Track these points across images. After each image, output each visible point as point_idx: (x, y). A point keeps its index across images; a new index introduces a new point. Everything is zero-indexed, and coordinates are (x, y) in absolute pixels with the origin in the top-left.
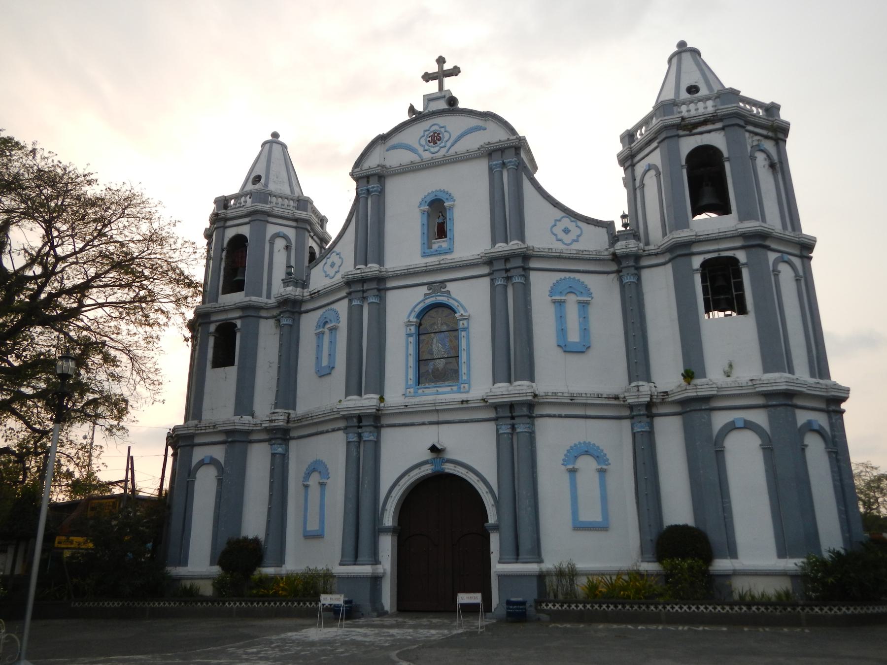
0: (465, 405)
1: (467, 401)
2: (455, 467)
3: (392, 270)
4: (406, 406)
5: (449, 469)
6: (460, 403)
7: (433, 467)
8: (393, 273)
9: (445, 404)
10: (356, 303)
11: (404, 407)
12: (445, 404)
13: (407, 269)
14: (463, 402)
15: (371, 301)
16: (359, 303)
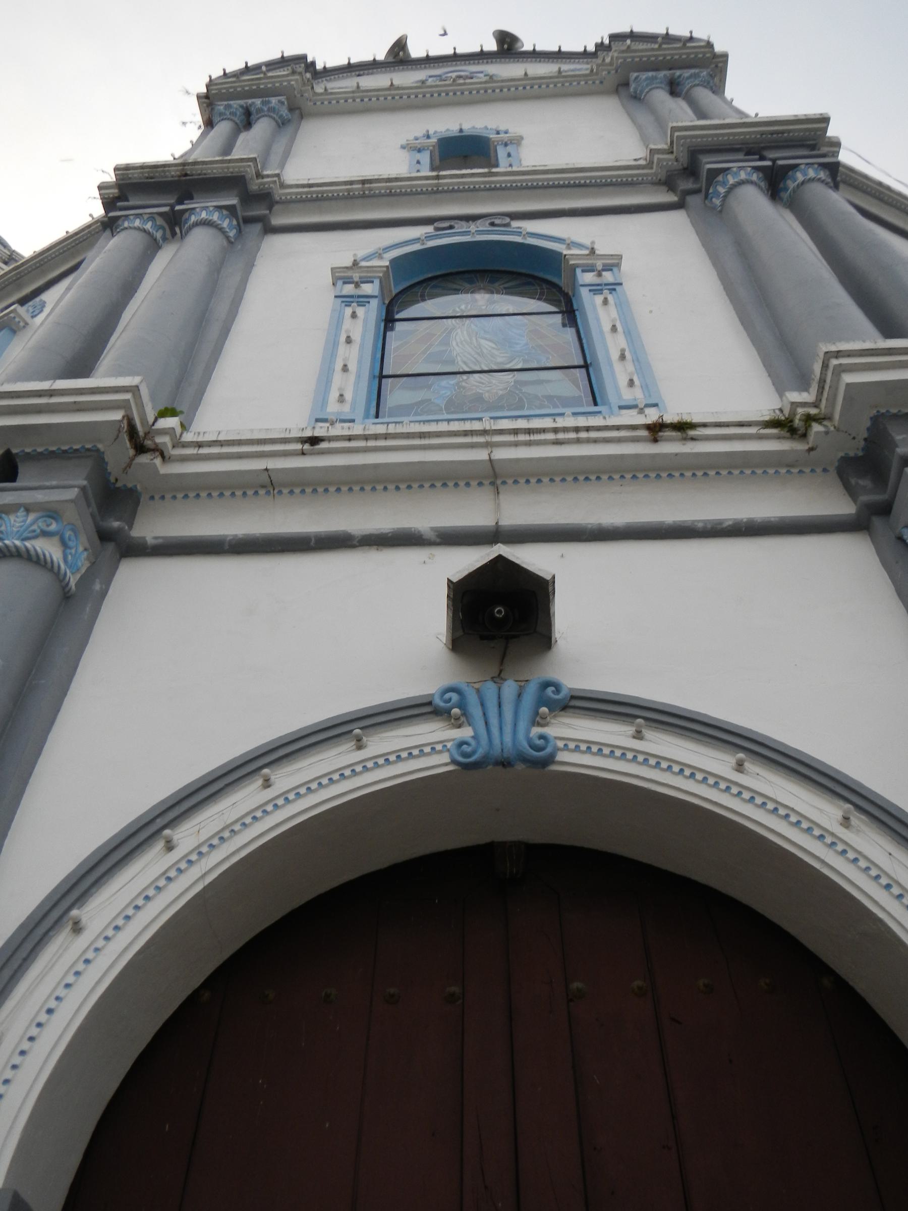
0: (670, 447)
1: (682, 427)
2: (638, 735)
3: (305, 182)
4: (314, 441)
5: (589, 747)
6: (644, 433)
7: (466, 733)
8: (306, 190)
9: (550, 436)
10: (137, 223)
11: (299, 446)
12: (550, 436)
13: (363, 182)
14: (656, 430)
15: (204, 215)
16: (148, 226)
